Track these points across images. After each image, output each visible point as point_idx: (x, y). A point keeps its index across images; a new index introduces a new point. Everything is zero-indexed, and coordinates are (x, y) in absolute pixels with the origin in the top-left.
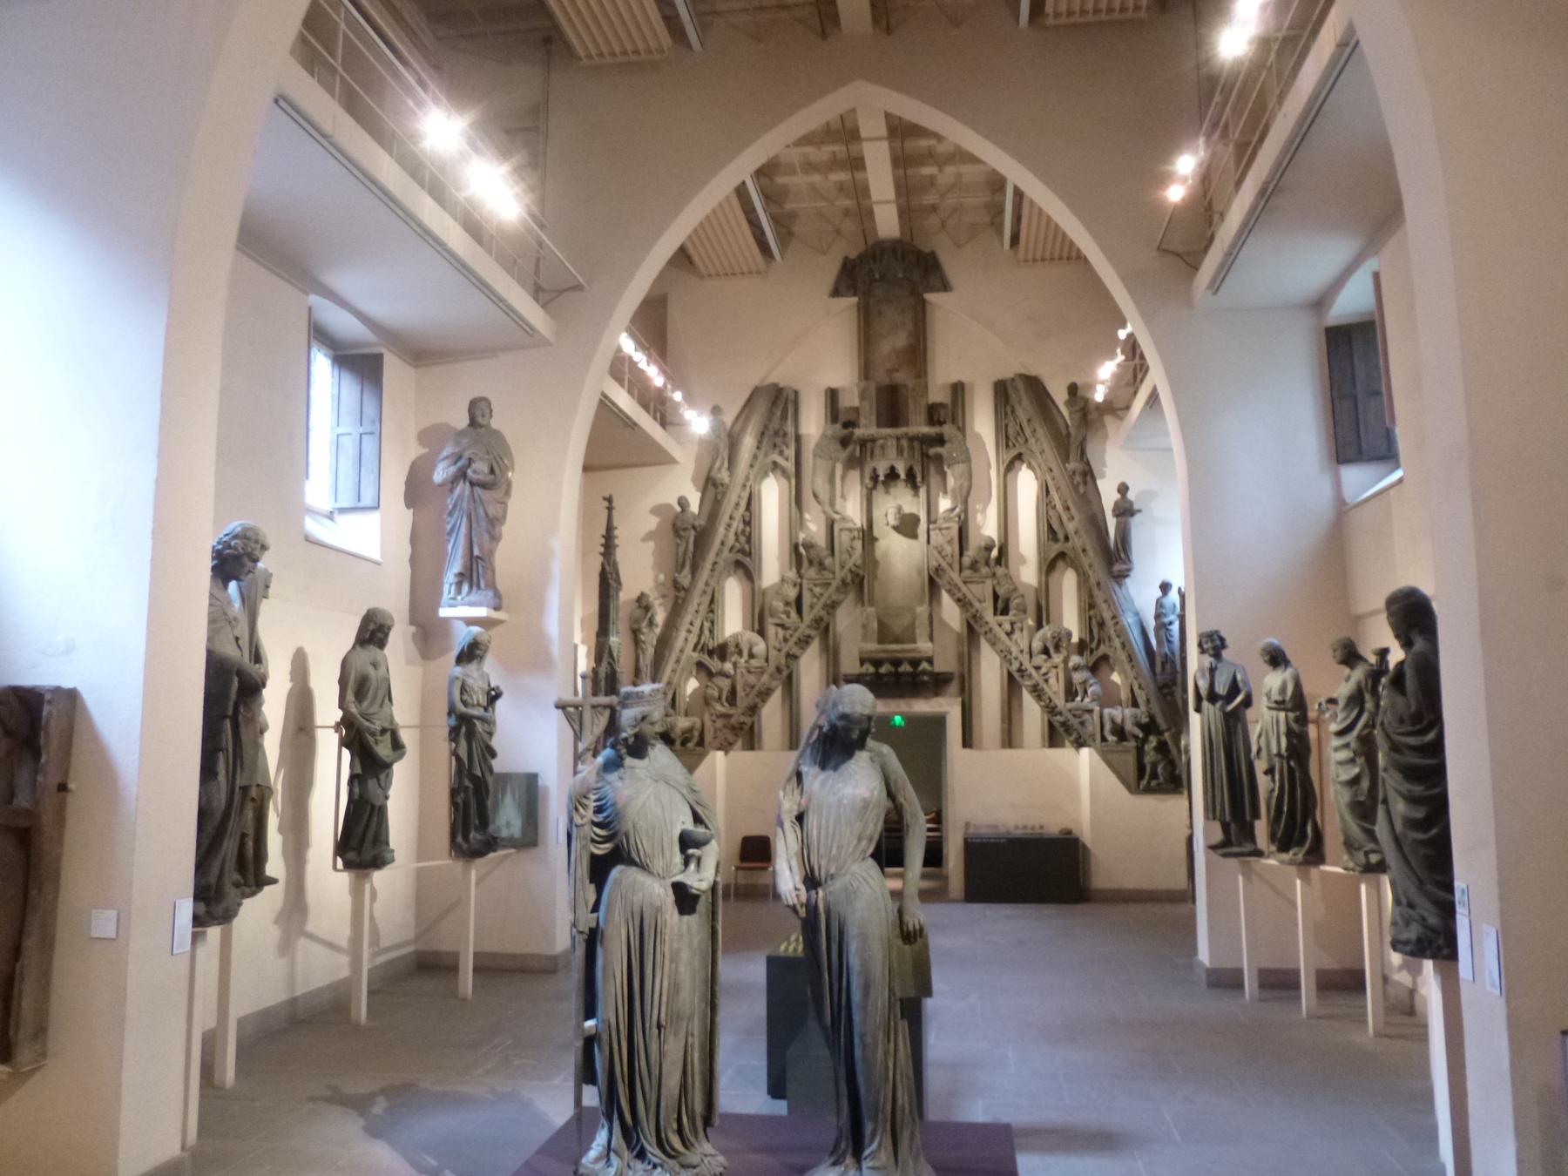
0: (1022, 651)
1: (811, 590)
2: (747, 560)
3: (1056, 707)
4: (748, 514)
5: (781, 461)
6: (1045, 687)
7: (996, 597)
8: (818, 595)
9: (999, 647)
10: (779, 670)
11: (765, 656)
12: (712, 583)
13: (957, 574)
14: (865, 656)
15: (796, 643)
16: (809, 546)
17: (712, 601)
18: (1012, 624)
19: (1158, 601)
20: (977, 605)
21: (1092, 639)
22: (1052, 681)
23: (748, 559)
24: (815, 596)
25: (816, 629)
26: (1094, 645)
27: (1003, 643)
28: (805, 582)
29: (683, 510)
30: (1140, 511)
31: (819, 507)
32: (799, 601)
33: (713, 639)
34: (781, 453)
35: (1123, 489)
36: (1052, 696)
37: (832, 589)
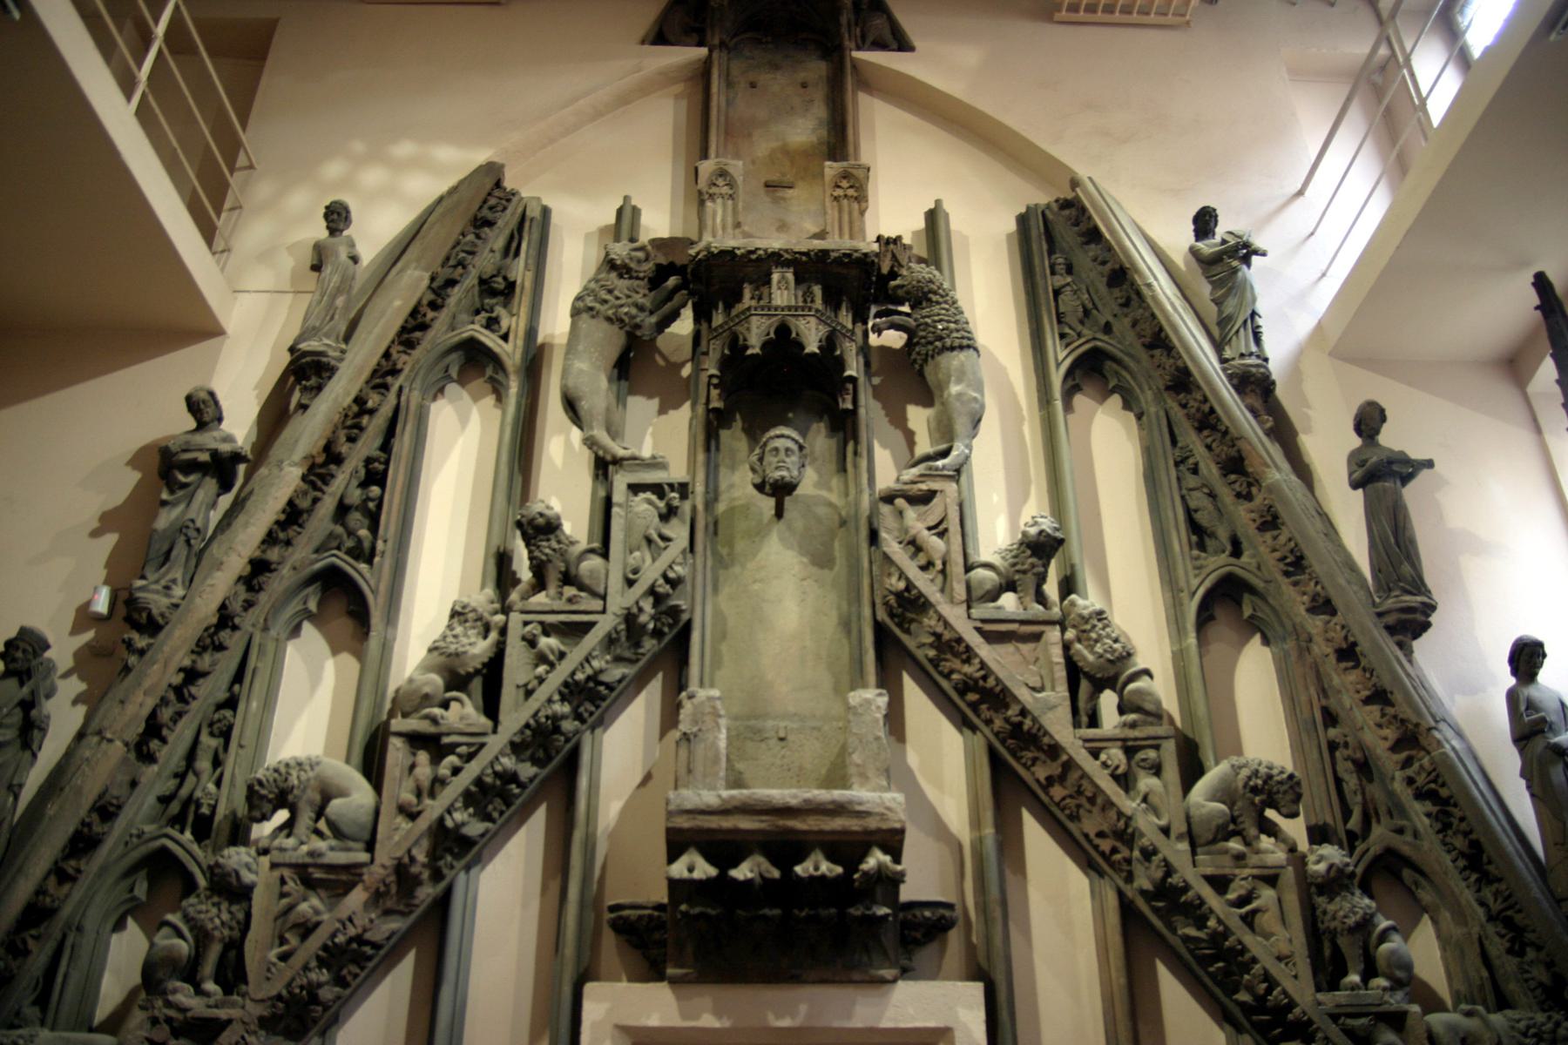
0: (1166, 831)
1: (531, 642)
2: (360, 572)
3: (1292, 1005)
4: (383, 456)
5: (490, 340)
6: (1249, 939)
7: (1074, 671)
8: (552, 657)
9: (1091, 824)
10: (403, 874)
11: (366, 836)
12: (247, 621)
13: (962, 610)
14: (684, 823)
15: (468, 798)
16: (540, 530)
17: (239, 677)
18: (1130, 751)
19: (1512, 697)
20: (1024, 695)
21: (1347, 814)
22: (1268, 920)
23: (363, 567)
24: (542, 659)
25: (535, 761)
26: (1354, 822)
27: (1109, 804)
28: (516, 618)
29: (201, 426)
30: (1429, 464)
31: (576, 434)
32: (494, 668)
33: (218, 784)
34: (492, 323)
35: (1369, 421)
36: (1277, 970)
37: (593, 639)
